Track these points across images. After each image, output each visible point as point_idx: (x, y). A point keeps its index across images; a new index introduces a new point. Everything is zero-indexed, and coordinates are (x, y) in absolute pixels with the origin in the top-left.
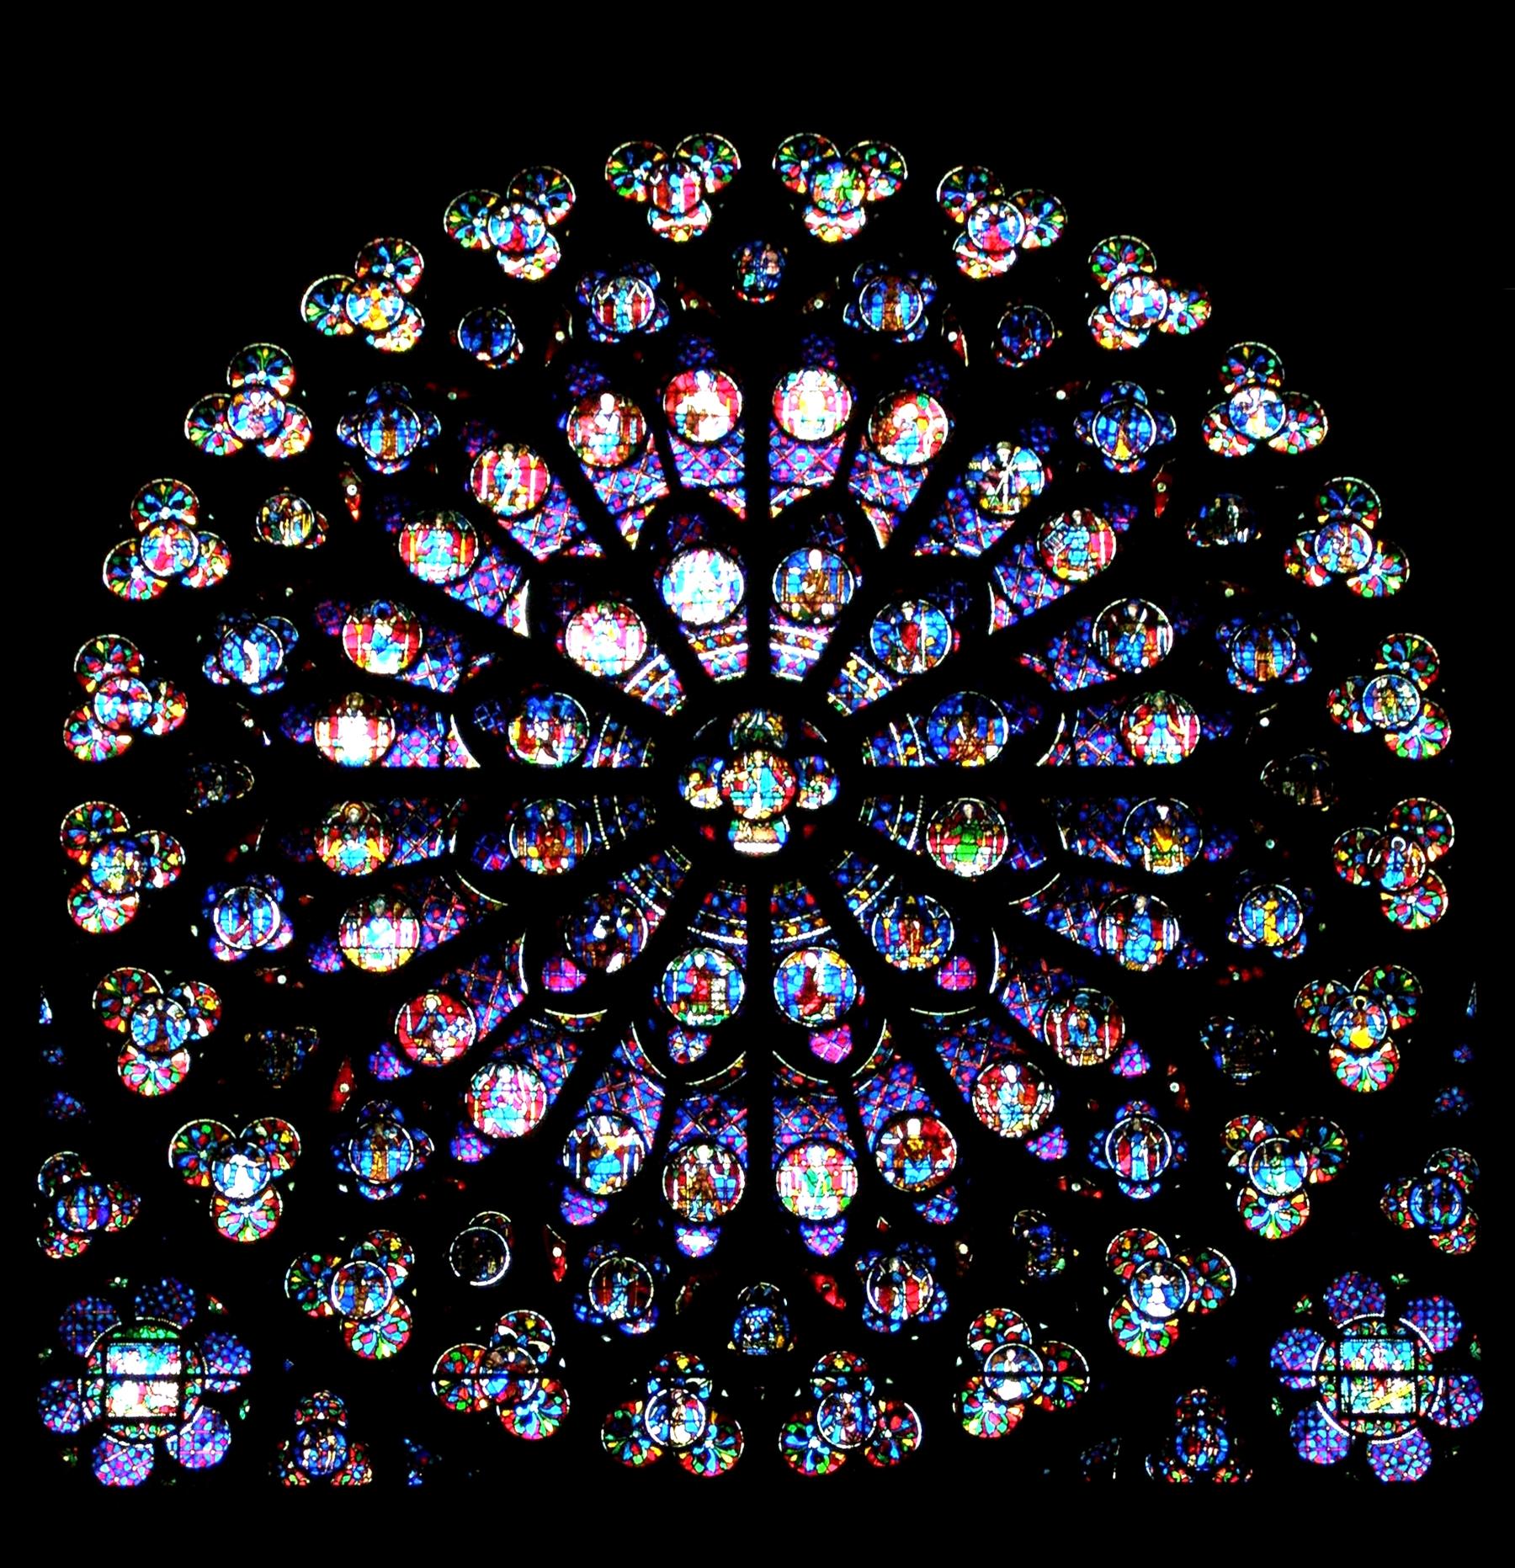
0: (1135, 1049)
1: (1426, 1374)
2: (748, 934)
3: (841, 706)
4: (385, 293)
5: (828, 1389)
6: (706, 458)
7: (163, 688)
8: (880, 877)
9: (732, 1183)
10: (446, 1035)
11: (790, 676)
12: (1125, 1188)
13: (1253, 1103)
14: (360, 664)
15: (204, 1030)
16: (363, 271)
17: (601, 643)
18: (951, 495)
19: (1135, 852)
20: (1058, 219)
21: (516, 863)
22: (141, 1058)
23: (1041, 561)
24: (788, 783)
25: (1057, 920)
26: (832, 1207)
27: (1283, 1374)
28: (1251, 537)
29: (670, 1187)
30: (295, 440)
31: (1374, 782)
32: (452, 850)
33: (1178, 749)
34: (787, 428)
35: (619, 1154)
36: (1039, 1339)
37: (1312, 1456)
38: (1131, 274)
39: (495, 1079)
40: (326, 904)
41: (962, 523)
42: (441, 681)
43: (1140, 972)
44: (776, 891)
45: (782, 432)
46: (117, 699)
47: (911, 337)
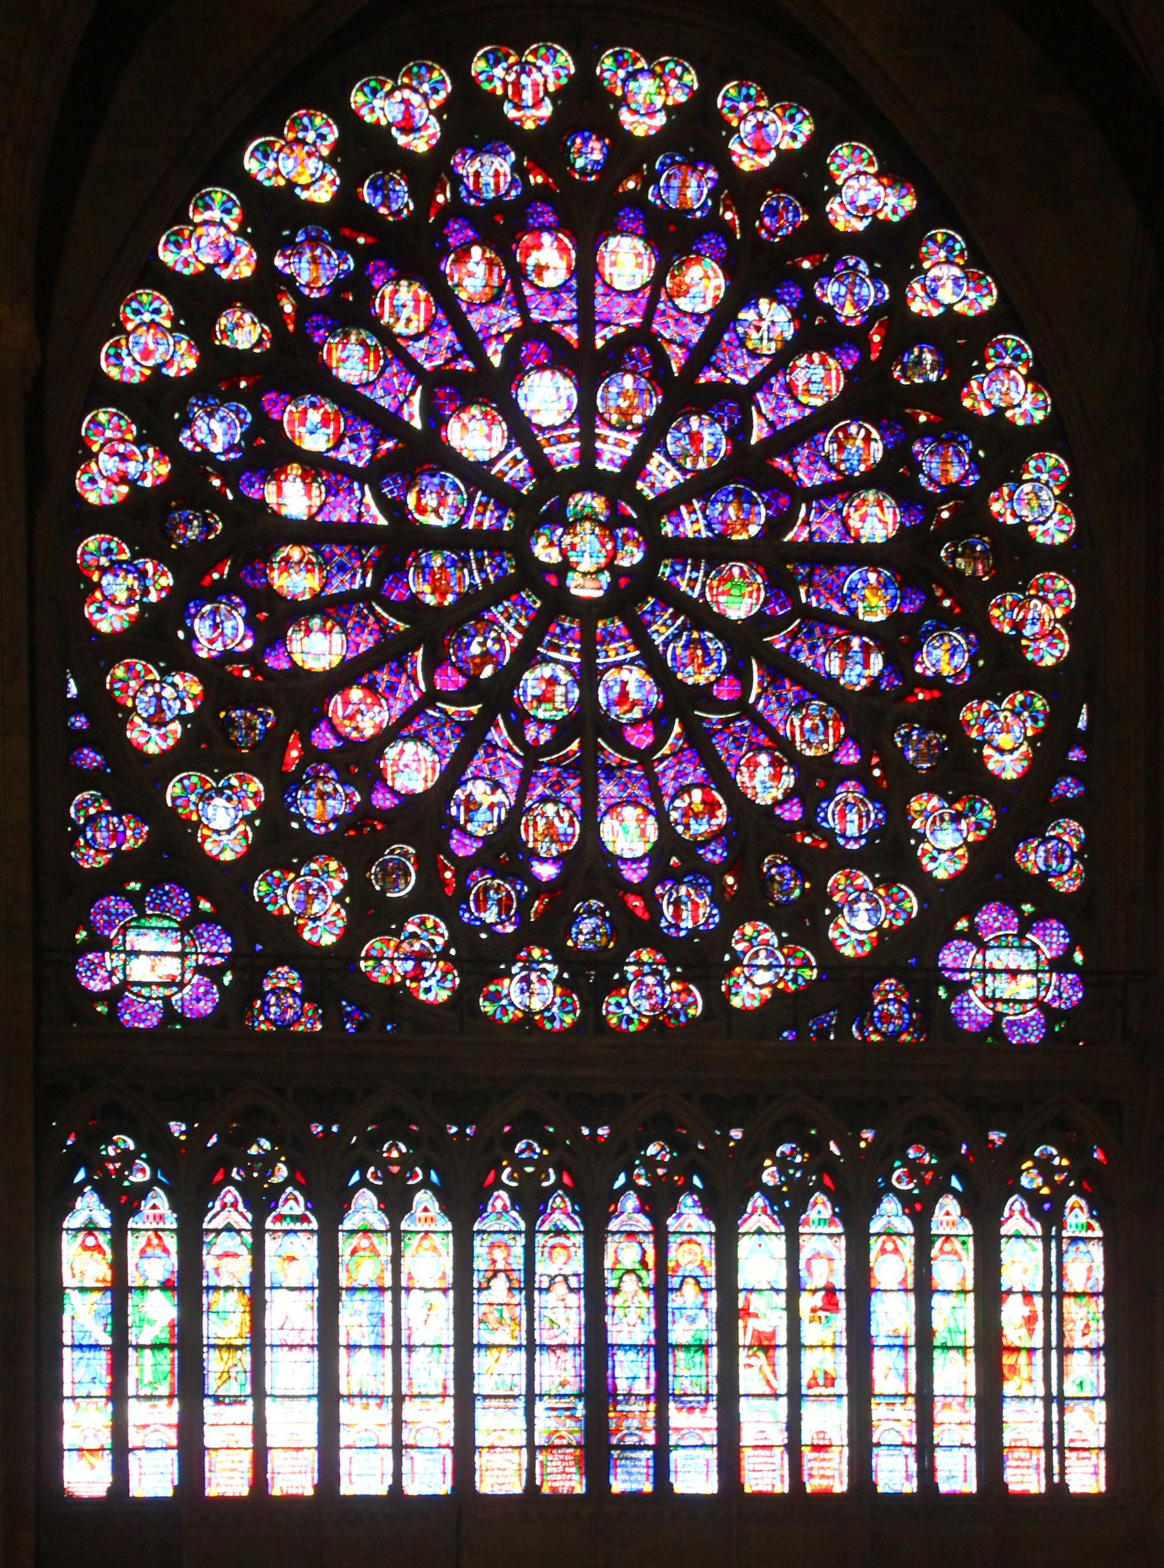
0: (850, 744)
1: (1044, 971)
2: (581, 653)
3: (646, 492)
4: (309, 155)
5: (639, 974)
6: (548, 299)
7: (151, 452)
8: (674, 617)
9: (570, 831)
10: (366, 718)
11: (610, 468)
12: (841, 841)
13: (930, 785)
14: (297, 442)
15: (190, 708)
16: (291, 136)
17: (474, 436)
18: (726, 337)
19: (852, 605)
20: (807, 128)
21: (414, 597)
22: (145, 726)
23: (789, 388)
24: (609, 546)
25: (797, 652)
26: (640, 849)
27: (948, 970)
28: (939, 377)
29: (527, 831)
30: (243, 268)
31: (1018, 558)
32: (368, 585)
33: (884, 533)
34: (607, 279)
35: (491, 807)
36: (782, 943)
37: (966, 1026)
38: (859, 173)
39: (402, 752)
40: (276, 618)
41: (734, 359)
42: (359, 458)
43: (853, 692)
44: (600, 625)
45: (605, 284)
46: (116, 458)
47: (698, 214)
